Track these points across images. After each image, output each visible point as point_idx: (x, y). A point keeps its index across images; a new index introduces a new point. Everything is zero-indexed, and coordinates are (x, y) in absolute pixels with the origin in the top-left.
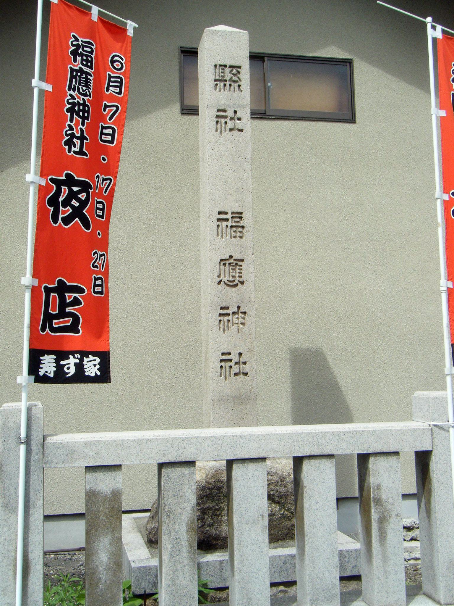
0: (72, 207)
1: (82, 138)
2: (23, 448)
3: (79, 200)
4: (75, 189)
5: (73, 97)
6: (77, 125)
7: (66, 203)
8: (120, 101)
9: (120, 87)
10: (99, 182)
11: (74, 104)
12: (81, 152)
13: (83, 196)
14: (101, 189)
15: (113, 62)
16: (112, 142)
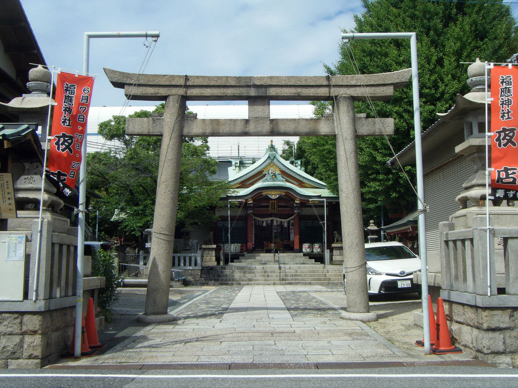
0: (65, 145)
1: (69, 120)
2: (39, 234)
3: (68, 143)
4: (66, 139)
5: (66, 105)
6: (67, 115)
7: (62, 144)
8: (86, 105)
9: (87, 100)
10: (77, 136)
11: (66, 108)
12: (69, 125)
13: (70, 141)
14: (78, 139)
15: (84, 91)
16: (83, 121)
